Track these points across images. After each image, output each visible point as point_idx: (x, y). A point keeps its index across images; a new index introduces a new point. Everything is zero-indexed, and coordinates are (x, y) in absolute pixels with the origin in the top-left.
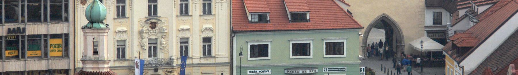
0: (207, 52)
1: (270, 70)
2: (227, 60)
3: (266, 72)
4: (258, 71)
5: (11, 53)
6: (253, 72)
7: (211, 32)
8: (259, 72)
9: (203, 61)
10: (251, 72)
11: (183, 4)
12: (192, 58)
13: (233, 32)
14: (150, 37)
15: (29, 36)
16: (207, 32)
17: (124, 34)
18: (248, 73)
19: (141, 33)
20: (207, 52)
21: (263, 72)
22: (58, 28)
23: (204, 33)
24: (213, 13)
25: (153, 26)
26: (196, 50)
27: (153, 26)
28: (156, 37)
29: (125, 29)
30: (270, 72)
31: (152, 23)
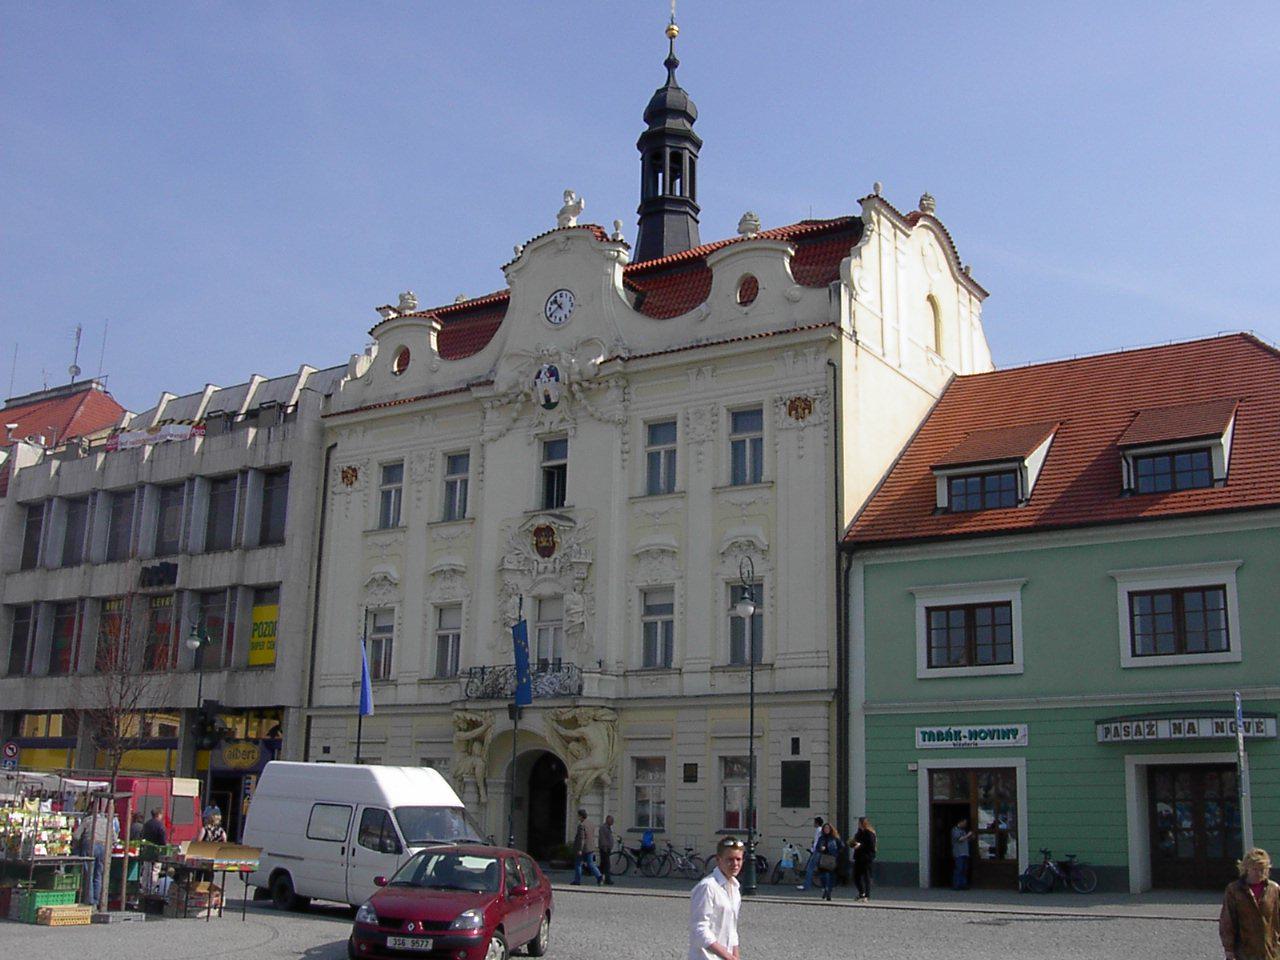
0: (746, 647)
1: (1022, 729)
2: (825, 678)
3: (1006, 734)
4: (965, 730)
6: (940, 737)
8: (973, 735)
10: (931, 736)
12: (680, 671)
18: (920, 743)
21: (991, 734)
23: (730, 561)
26: (700, 636)
28: (559, 590)
30: (1022, 740)
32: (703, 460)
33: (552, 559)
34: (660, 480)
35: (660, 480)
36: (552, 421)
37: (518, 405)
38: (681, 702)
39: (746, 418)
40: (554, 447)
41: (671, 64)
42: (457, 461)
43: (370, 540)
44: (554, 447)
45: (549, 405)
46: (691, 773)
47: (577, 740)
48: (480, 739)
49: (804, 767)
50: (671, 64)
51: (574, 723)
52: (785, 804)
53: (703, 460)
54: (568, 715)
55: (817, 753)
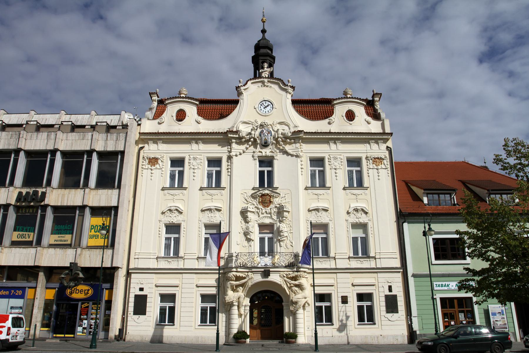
0: (361, 247)
2: (397, 263)
5: (22, 236)
6: (442, 286)
7: (364, 215)
9: (355, 264)
11: (315, 171)
12: (335, 259)
13: (403, 217)
14: (261, 221)
15: (56, 209)
16: (359, 215)
17: (217, 214)
19: (244, 213)
20: (361, 247)
22: (104, 197)
24: (366, 185)
25: (265, 200)
27: (265, 200)
29: (219, 205)
31: (263, 195)
32: (337, 175)
33: (269, 208)
34: (318, 180)
35: (318, 180)
36: (267, 152)
37: (250, 143)
38: (336, 270)
39: (354, 162)
40: (266, 162)
41: (264, 31)
42: (214, 162)
43: (166, 191)
44: (266, 162)
45: (265, 145)
46: (345, 300)
47: (296, 286)
48: (242, 285)
49: (395, 297)
50: (264, 31)
51: (295, 278)
52: (388, 312)
53: (337, 175)
54: (293, 275)
55: (398, 291)
